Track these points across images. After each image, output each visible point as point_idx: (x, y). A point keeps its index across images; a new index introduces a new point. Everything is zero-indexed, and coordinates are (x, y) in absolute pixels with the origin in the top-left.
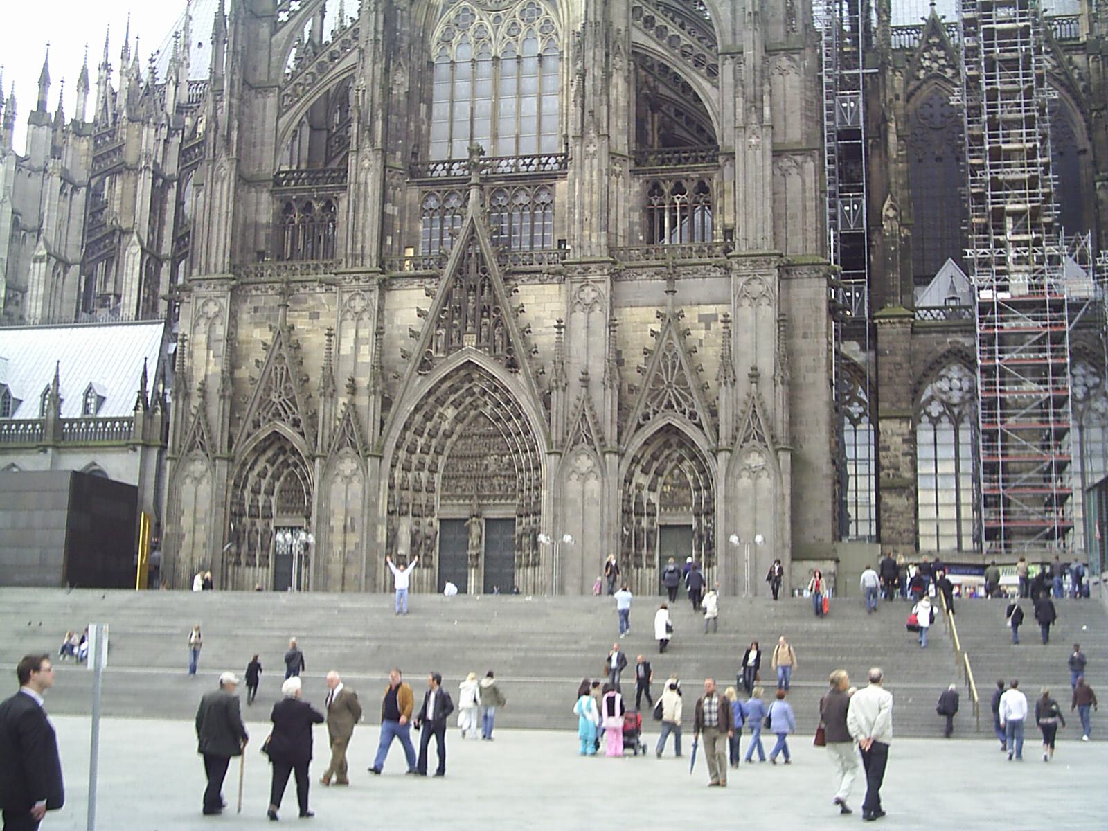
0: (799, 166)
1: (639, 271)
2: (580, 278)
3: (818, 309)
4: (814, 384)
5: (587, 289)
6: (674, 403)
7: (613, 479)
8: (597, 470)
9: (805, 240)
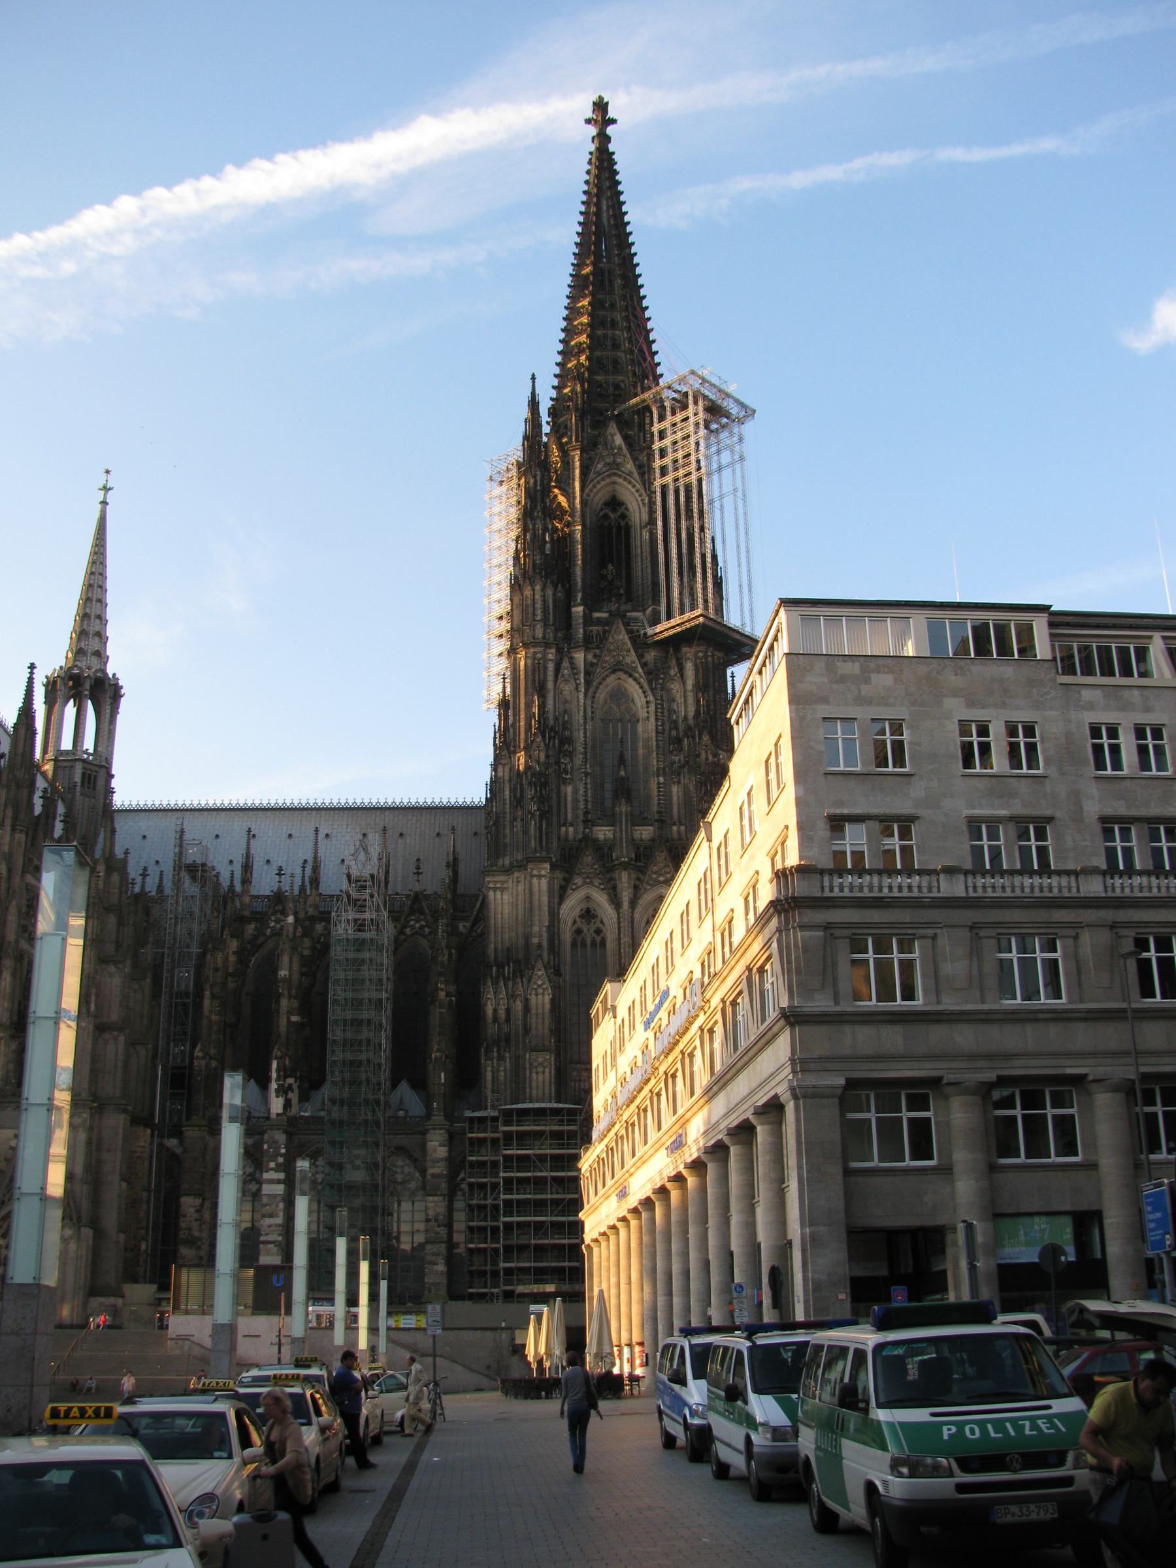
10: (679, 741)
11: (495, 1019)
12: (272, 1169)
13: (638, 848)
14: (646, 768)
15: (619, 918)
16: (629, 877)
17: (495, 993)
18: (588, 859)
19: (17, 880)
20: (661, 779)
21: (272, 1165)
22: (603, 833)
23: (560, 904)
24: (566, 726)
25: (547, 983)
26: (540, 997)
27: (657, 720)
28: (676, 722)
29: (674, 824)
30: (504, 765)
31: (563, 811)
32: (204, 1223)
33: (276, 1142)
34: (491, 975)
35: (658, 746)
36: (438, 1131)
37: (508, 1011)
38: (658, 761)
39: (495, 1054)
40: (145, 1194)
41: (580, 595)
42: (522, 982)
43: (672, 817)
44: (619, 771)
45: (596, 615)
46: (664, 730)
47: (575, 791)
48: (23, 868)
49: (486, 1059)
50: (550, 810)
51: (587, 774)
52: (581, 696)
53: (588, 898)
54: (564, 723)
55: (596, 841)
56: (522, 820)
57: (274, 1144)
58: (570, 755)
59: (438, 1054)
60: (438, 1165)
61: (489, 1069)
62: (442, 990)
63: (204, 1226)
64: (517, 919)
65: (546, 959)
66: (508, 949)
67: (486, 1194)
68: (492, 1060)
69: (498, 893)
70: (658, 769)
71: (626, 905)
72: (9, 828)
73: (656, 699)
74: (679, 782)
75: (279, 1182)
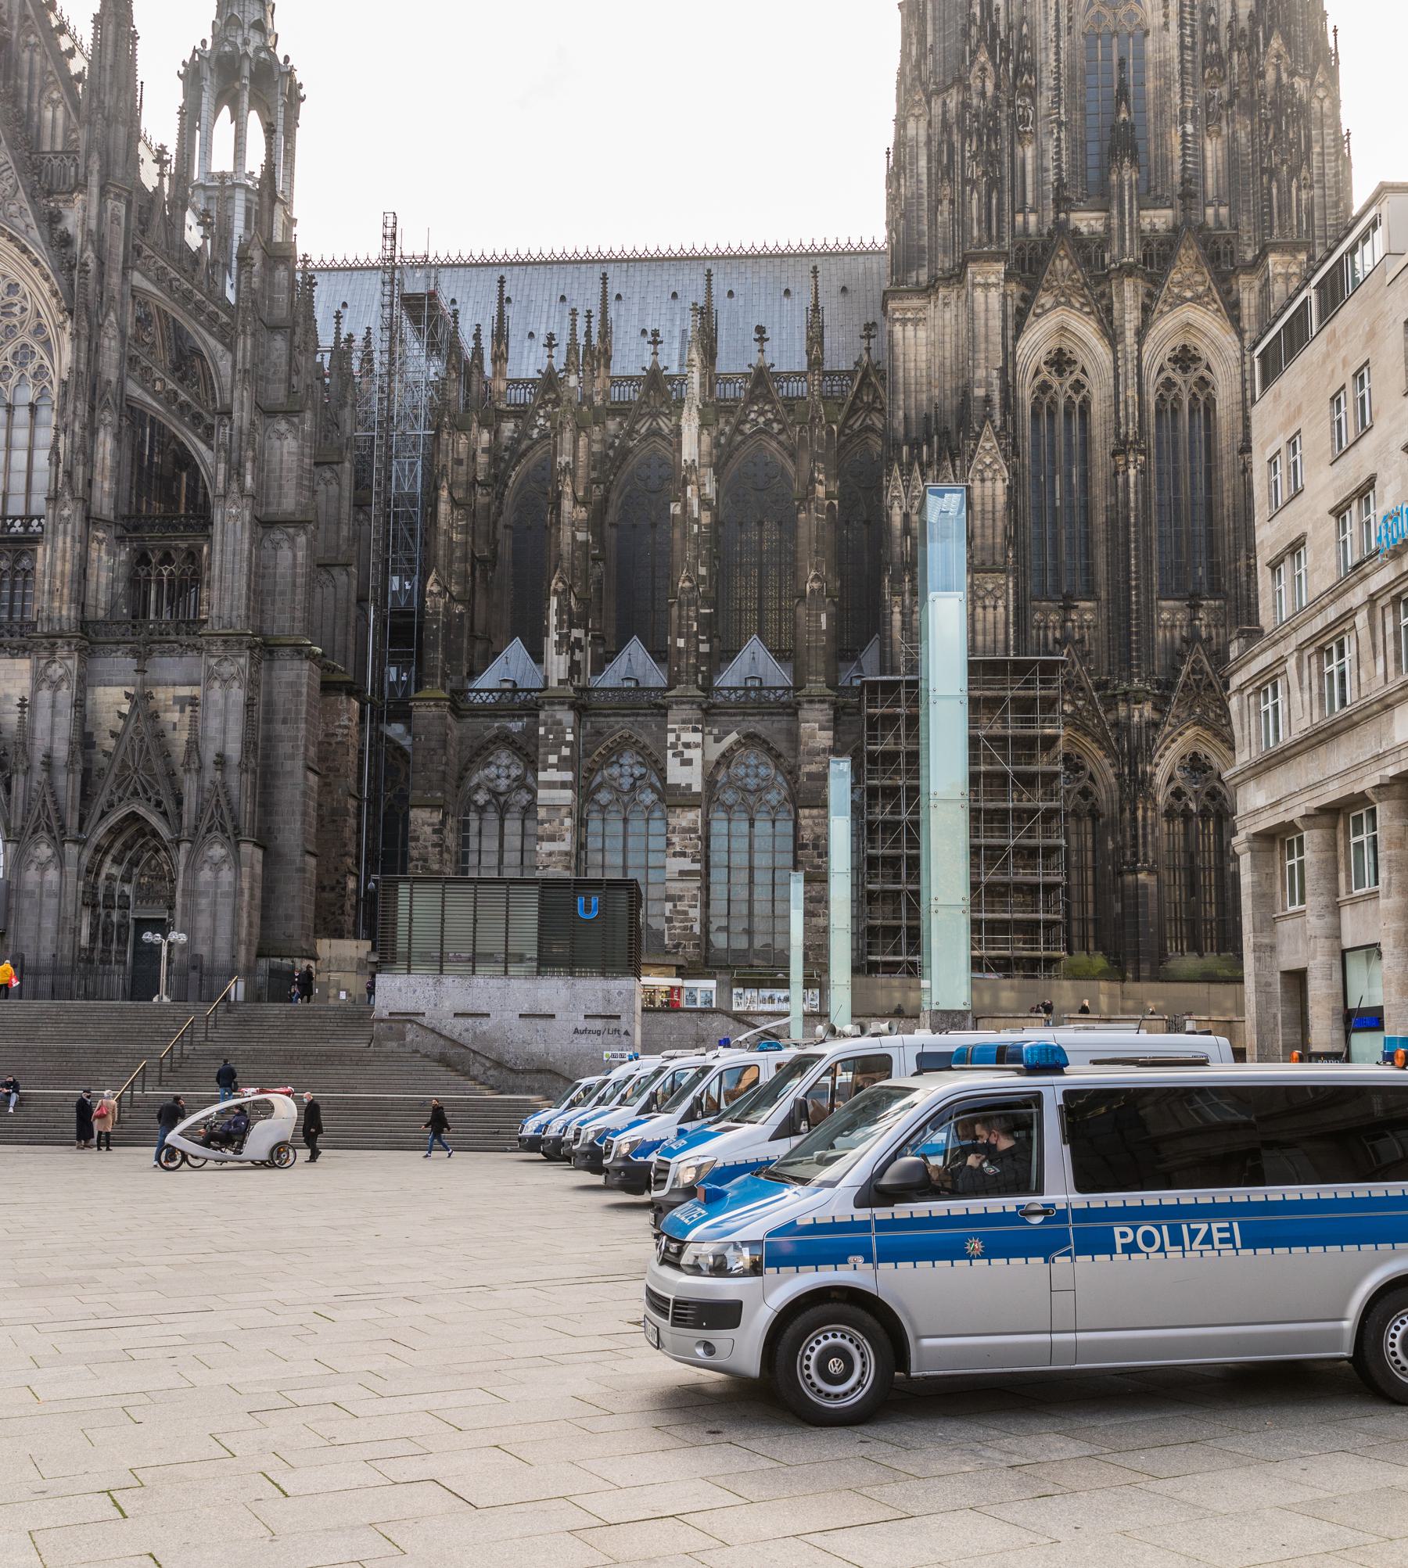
0: (292, 540)
1: (114, 647)
2: (45, 654)
3: (299, 694)
4: (291, 773)
5: (55, 666)
6: (140, 789)
7: (71, 869)
8: (56, 860)
9: (293, 619)
10: (1218, 61)
12: (552, 766)
13: (1148, 245)
14: (1160, 113)
15: (1116, 360)
16: (1136, 291)
17: (906, 488)
18: (1062, 265)
19: (115, 279)
20: (1190, 128)
21: (553, 759)
22: (1086, 221)
23: (1016, 338)
25: (1001, 461)
26: (988, 484)
27: (1182, 26)
28: (1215, 29)
29: (1211, 204)
30: (918, 117)
32: (448, 850)
33: (559, 723)
34: (900, 459)
35: (1183, 71)
36: (817, 706)
38: (1183, 97)
39: (907, 586)
42: (954, 466)
43: (1205, 192)
44: (1118, 113)
46: (1194, 43)
47: (1040, 154)
48: (125, 261)
49: (893, 594)
51: (1060, 124)
53: (1063, 329)
54: (1021, 38)
55: (1076, 231)
56: (952, 202)
58: (1032, 92)
59: (816, 585)
60: (818, 759)
61: (897, 609)
62: (821, 482)
63: (446, 856)
64: (943, 364)
65: (998, 423)
66: (927, 417)
67: (897, 806)
68: (902, 594)
69: (910, 327)
70: (1183, 111)
71: (1130, 337)
72: (95, 190)
74: (1219, 134)
75: (564, 785)
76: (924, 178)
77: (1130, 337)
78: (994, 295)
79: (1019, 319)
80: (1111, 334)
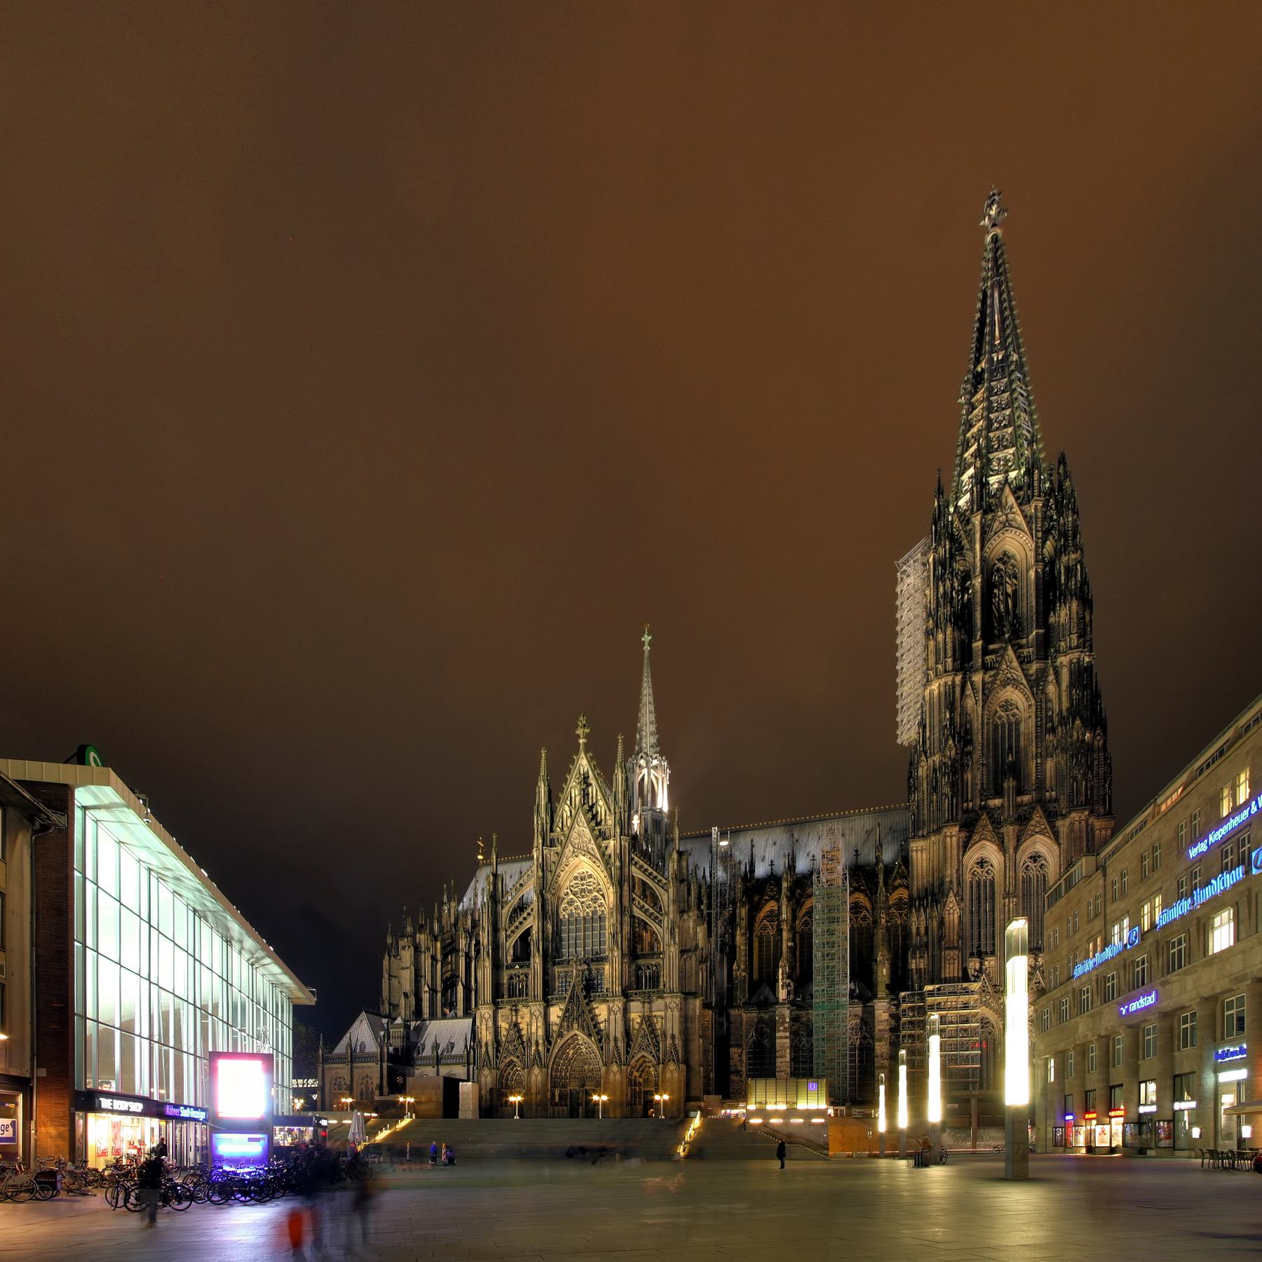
11: (918, 933)
14: (1027, 755)
17: (918, 918)
23: (963, 855)
24: (968, 732)
27: (1037, 717)
28: (1051, 717)
29: (1047, 791)
31: (965, 794)
37: (927, 928)
38: (1037, 748)
40: (711, 1046)
41: (979, 633)
45: (991, 647)
46: (1042, 724)
50: (958, 788)
51: (983, 764)
52: (980, 709)
57: (783, 1017)
70: (1036, 754)
73: (1037, 702)
76: (925, 792)
77: (1011, 851)
78: (954, 839)
79: (965, 846)
80: (1002, 848)
